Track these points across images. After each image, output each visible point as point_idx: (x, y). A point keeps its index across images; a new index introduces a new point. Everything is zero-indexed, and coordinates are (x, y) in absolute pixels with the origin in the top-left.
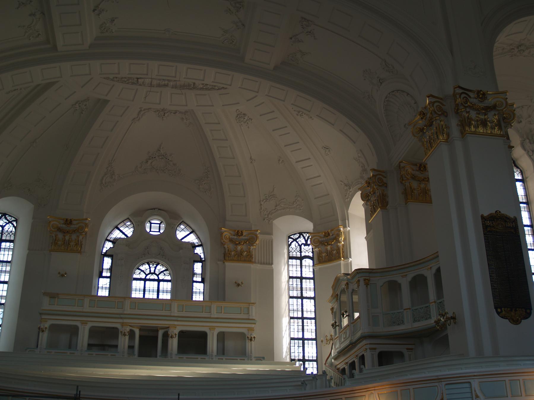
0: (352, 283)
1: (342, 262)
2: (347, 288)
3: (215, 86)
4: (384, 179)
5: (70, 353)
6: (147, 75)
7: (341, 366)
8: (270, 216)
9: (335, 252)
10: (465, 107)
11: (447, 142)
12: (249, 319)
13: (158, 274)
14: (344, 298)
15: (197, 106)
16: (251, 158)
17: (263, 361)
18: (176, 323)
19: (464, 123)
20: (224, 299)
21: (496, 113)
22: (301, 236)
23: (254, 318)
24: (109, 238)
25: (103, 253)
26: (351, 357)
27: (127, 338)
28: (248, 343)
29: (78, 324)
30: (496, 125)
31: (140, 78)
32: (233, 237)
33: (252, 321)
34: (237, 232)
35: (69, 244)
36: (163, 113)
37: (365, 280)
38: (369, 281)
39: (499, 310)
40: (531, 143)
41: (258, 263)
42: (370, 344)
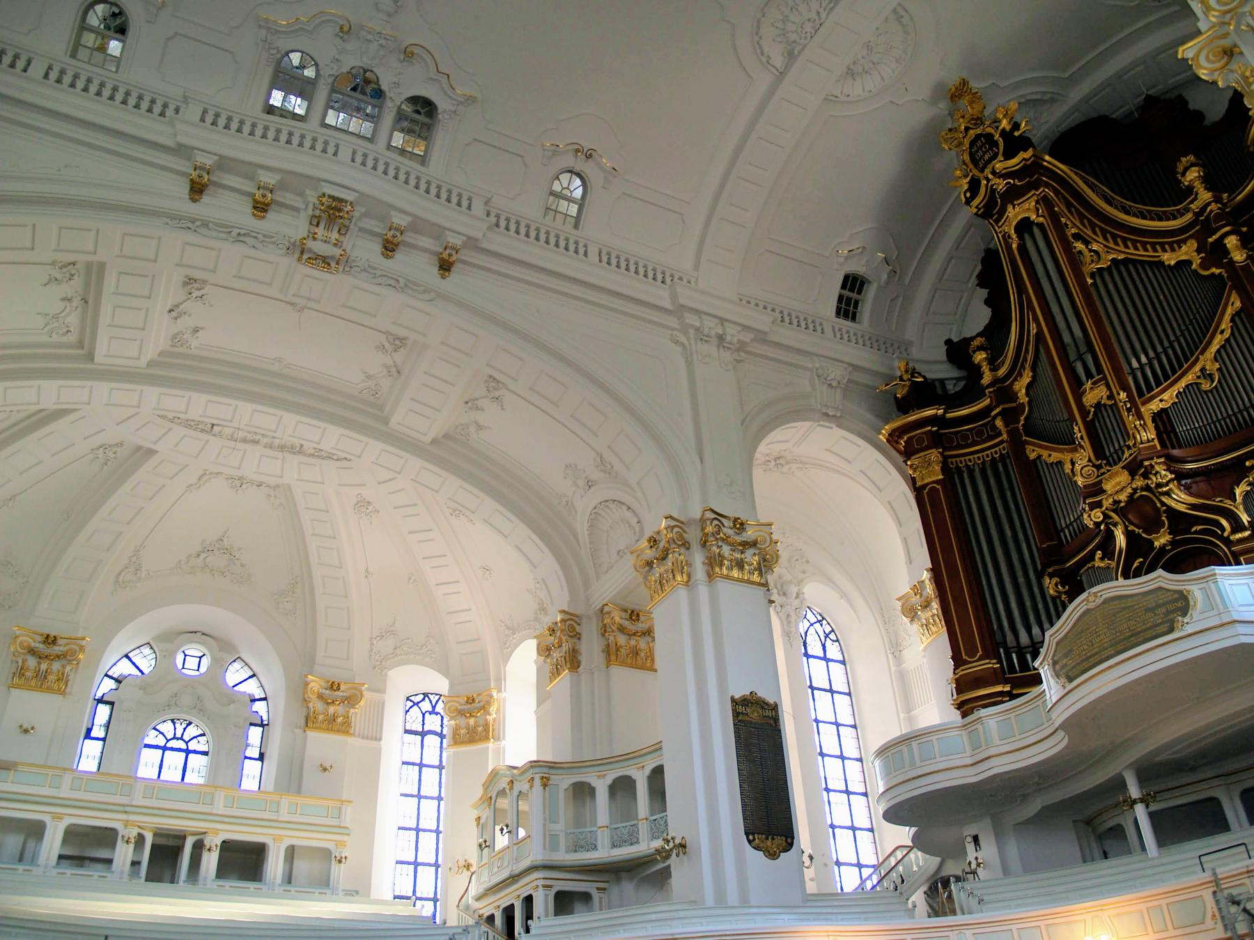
0: (520, 781)
1: (491, 745)
2: (511, 788)
3: (334, 454)
4: (577, 627)
5: (24, 870)
6: (231, 421)
7: (487, 912)
8: (383, 663)
9: (480, 729)
10: (717, 539)
11: (687, 586)
12: (340, 827)
13: (187, 740)
14: (503, 803)
15: (298, 480)
16: (367, 570)
17: (357, 898)
18: (219, 826)
19: (713, 562)
20: (299, 791)
21: (757, 552)
22: (426, 698)
23: (347, 825)
24: (109, 673)
25: (96, 698)
26: (512, 896)
27: (132, 846)
28: (335, 866)
29: (46, 818)
30: (755, 570)
31: (218, 425)
32: (324, 691)
33: (343, 829)
34: (332, 685)
35: (45, 677)
36: (239, 482)
37: (542, 778)
38: (548, 780)
39: (751, 837)
40: (779, 595)
41: (359, 736)
42: (544, 879)
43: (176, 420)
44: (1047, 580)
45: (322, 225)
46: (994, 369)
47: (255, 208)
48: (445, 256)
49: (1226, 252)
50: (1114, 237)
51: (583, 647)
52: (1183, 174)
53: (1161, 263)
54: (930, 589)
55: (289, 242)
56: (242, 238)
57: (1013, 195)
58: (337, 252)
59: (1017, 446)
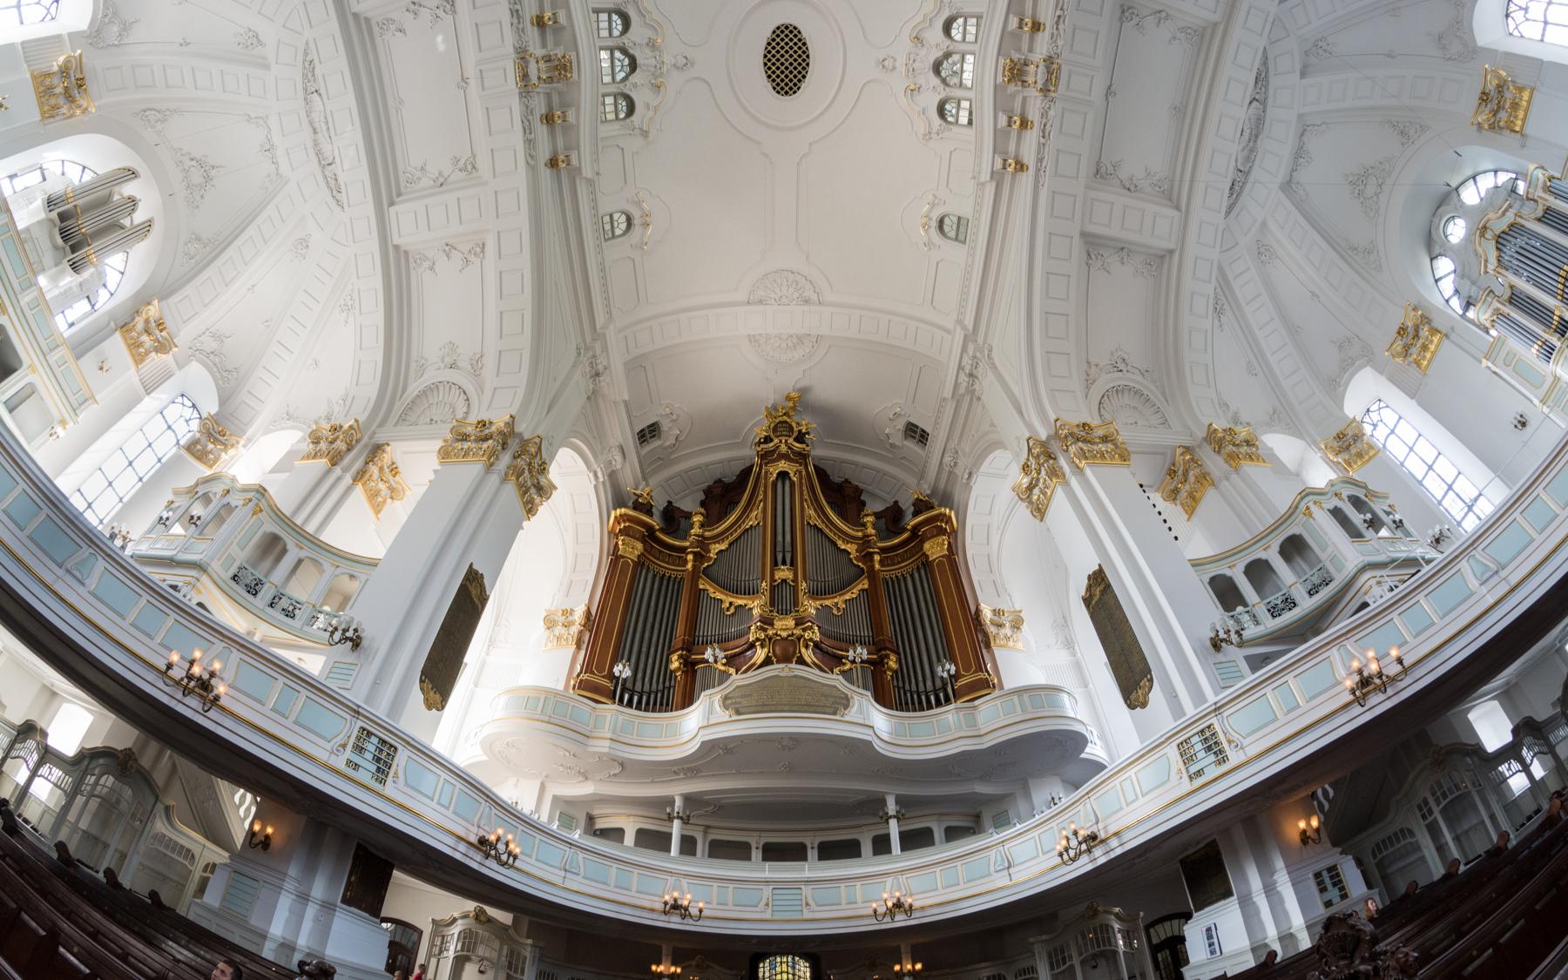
49: (872, 560)
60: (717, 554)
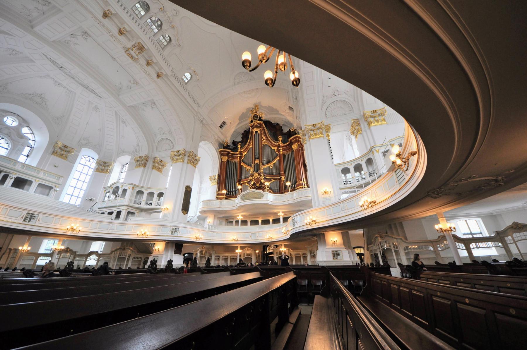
37: (133, 187)
43: (49, 59)
44: (237, 183)
45: (136, 48)
46: (241, 149)
47: (119, 31)
48: (160, 74)
49: (280, 151)
50: (267, 141)
51: (148, 164)
52: (279, 138)
53: (271, 148)
54: (217, 177)
55: (125, 46)
56: (112, 36)
57: (257, 127)
58: (137, 57)
59: (240, 162)
60: (245, 155)
